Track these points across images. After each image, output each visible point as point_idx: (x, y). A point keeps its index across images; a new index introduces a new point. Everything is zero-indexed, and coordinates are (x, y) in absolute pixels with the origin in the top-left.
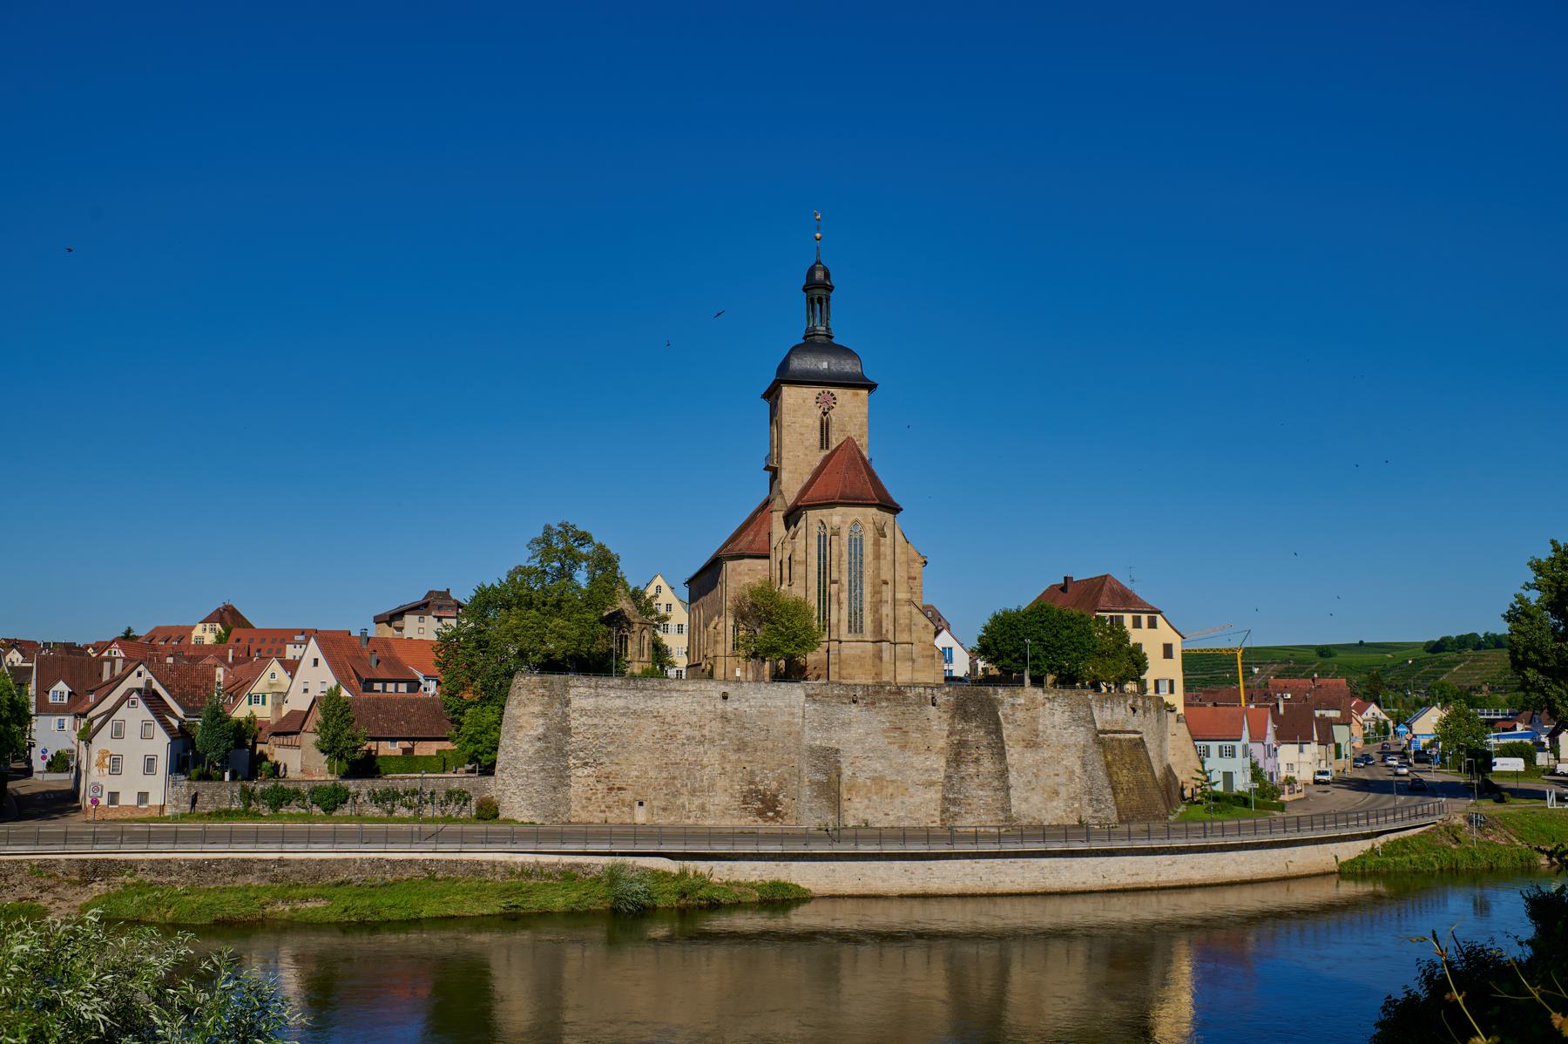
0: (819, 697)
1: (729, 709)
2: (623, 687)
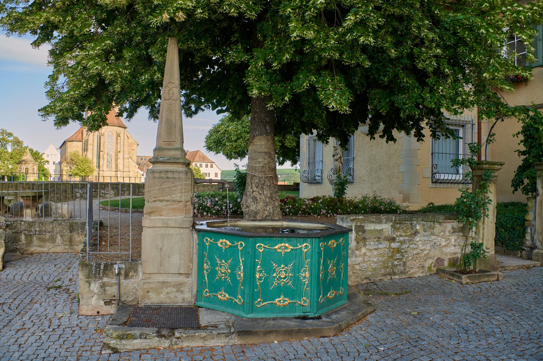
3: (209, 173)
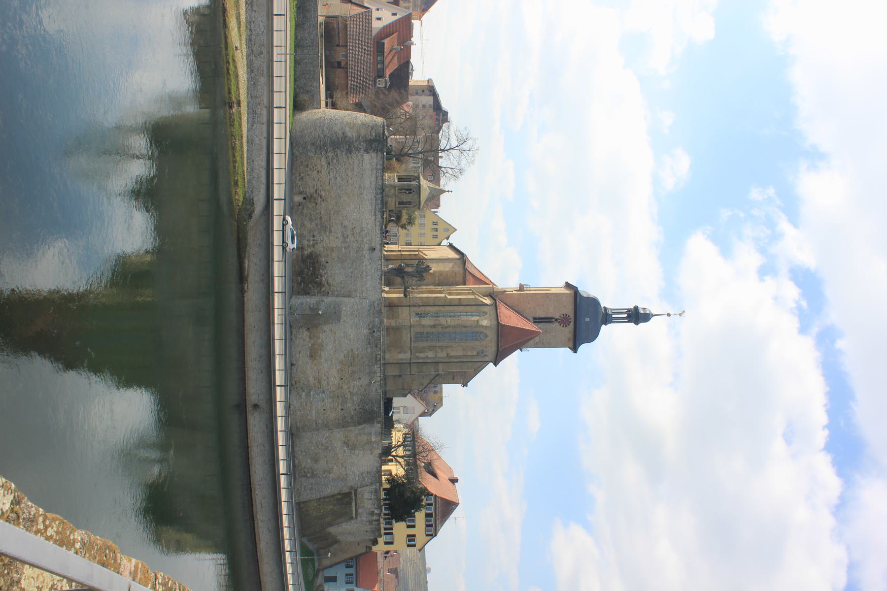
1: (365, 253)
2: (377, 186)
3: (414, 526)
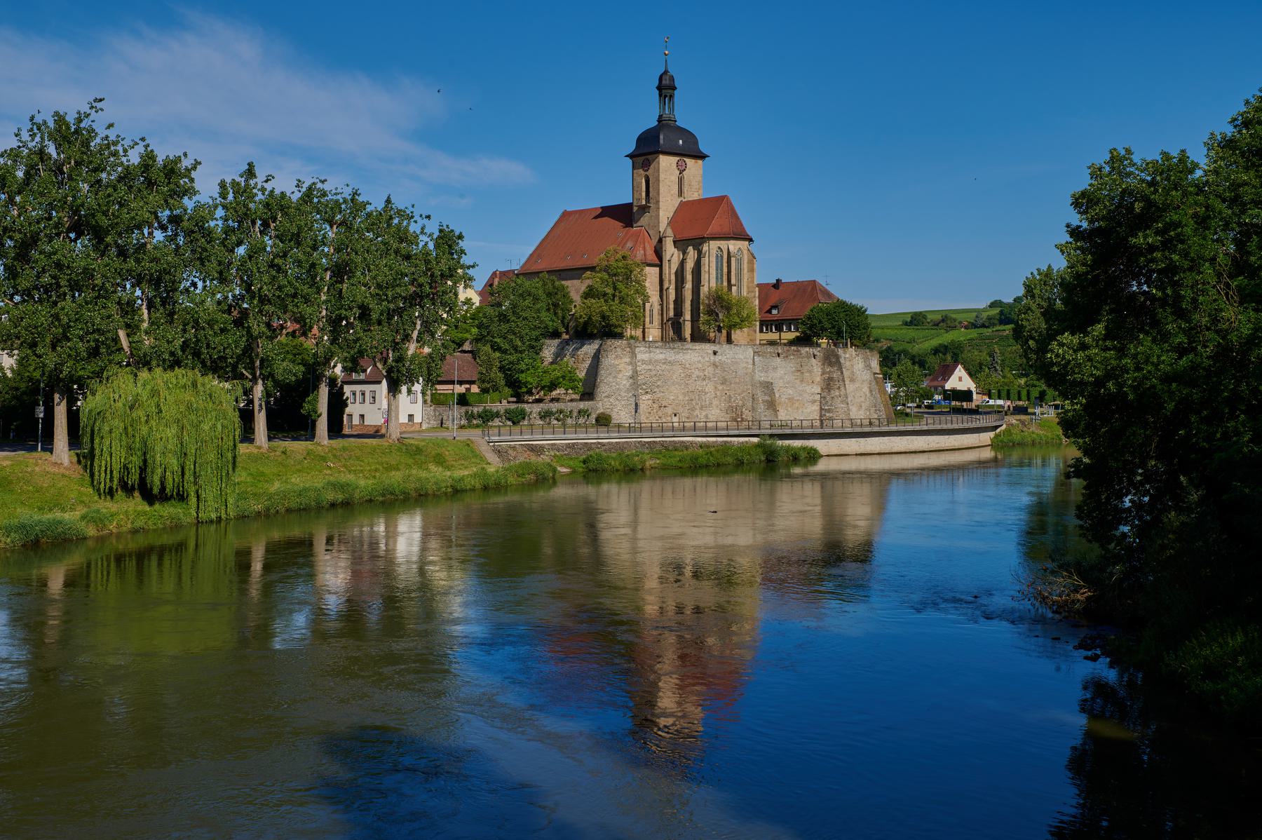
0: (760, 353)
1: (717, 360)
